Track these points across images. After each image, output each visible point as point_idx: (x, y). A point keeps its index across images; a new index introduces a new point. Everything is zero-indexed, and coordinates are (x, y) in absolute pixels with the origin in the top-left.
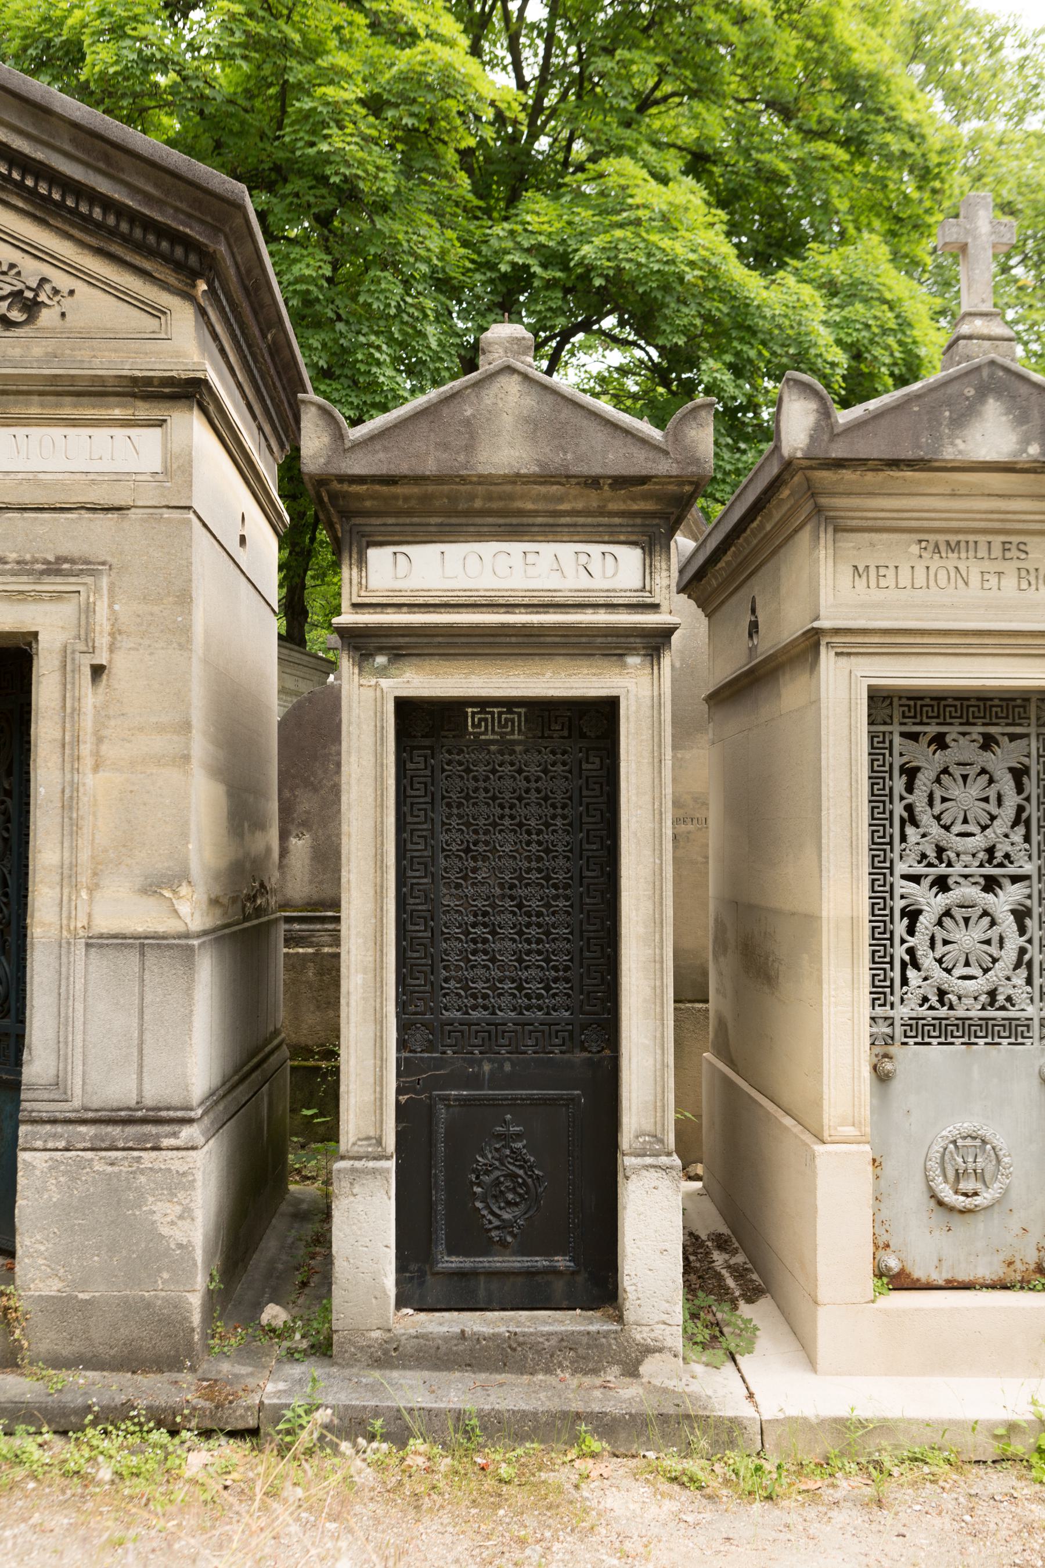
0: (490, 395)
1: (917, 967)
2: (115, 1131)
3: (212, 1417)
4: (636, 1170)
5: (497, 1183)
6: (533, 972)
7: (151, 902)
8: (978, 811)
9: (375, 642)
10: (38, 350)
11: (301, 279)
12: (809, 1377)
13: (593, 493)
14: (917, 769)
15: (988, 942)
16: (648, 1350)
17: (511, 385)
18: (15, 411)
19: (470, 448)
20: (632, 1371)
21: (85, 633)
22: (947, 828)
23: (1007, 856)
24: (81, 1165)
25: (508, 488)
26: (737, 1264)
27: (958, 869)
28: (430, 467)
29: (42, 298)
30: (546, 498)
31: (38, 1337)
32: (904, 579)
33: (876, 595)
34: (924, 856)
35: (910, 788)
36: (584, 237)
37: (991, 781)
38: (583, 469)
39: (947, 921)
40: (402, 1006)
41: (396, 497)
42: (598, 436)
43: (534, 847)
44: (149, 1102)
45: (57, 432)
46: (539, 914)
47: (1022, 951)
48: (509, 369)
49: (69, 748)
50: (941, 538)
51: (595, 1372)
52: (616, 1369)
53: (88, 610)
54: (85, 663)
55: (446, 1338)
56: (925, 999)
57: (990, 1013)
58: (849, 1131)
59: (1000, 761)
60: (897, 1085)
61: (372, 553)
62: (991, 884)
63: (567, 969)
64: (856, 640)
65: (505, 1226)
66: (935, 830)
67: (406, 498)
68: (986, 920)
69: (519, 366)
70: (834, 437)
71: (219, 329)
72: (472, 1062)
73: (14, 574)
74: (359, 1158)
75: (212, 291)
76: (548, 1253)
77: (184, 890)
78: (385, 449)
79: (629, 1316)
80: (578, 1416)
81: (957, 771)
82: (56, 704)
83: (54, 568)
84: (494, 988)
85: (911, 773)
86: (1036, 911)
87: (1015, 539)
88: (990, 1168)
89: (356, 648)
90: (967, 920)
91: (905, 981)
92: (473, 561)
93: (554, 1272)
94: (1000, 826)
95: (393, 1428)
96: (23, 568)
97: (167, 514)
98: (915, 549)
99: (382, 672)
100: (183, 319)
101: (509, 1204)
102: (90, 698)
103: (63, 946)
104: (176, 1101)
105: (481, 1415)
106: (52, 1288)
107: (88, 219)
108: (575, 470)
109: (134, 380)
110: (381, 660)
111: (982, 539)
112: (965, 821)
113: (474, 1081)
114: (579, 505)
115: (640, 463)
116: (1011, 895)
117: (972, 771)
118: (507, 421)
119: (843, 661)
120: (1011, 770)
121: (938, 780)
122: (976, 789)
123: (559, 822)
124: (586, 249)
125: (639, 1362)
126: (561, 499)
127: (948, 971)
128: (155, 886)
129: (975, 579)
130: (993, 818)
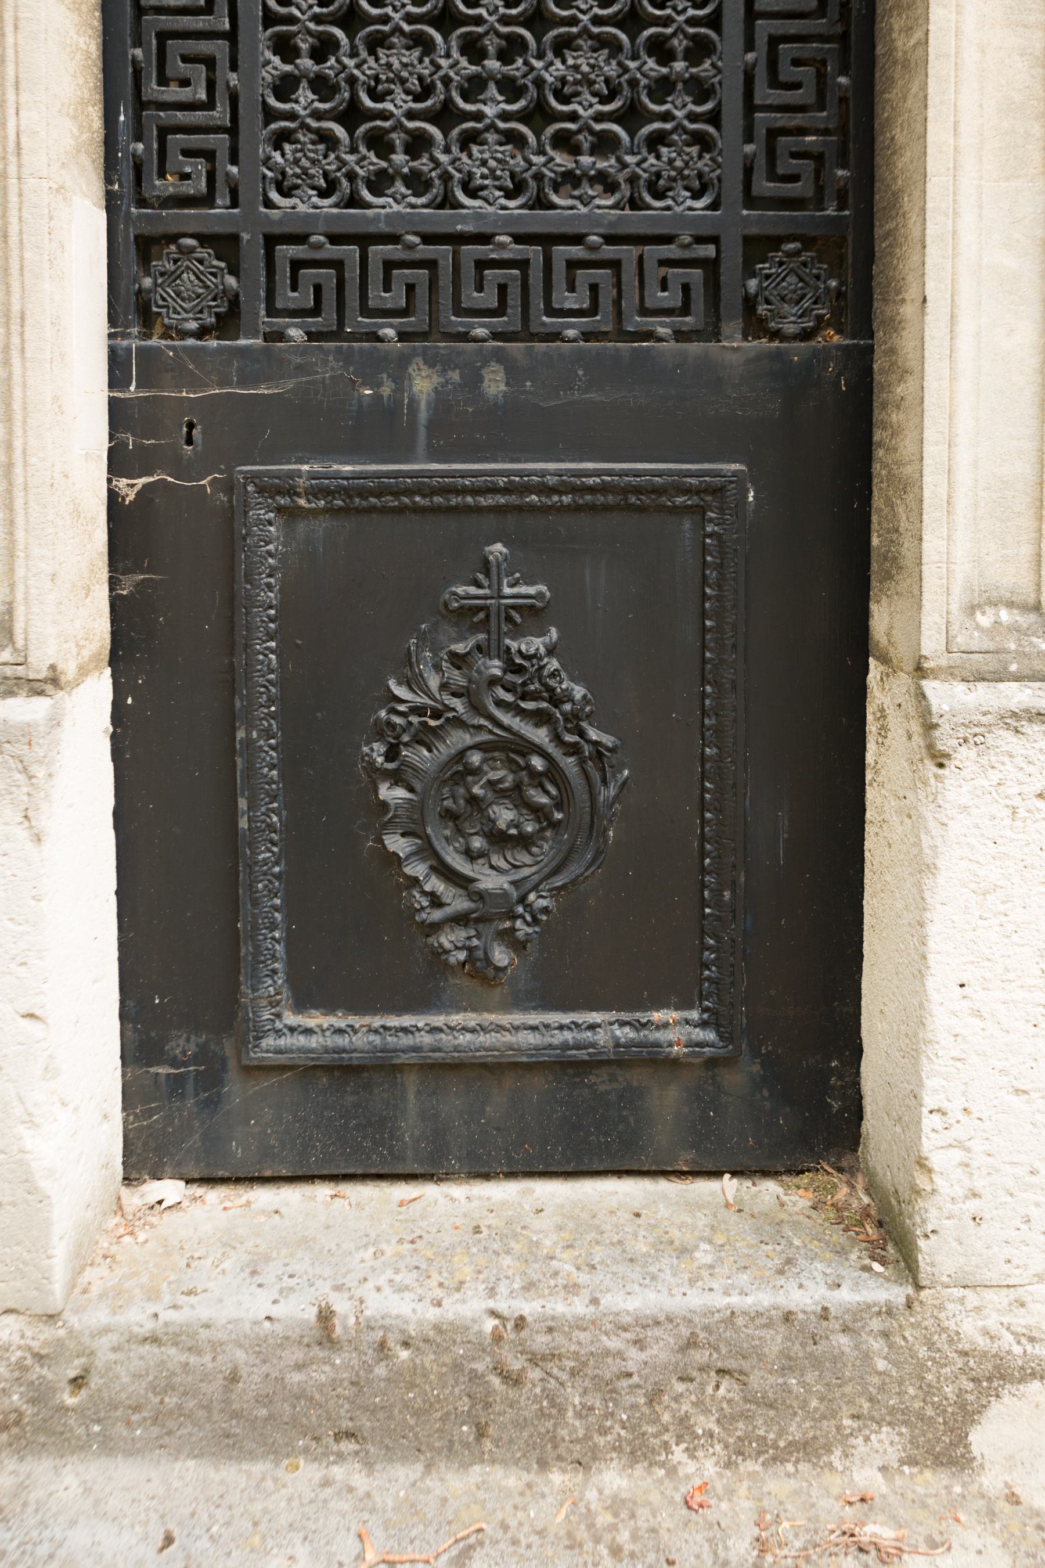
5: (458, 770)
65: (484, 913)
72: (372, 368)
76: (632, 996)
93: (654, 1060)
101: (499, 839)
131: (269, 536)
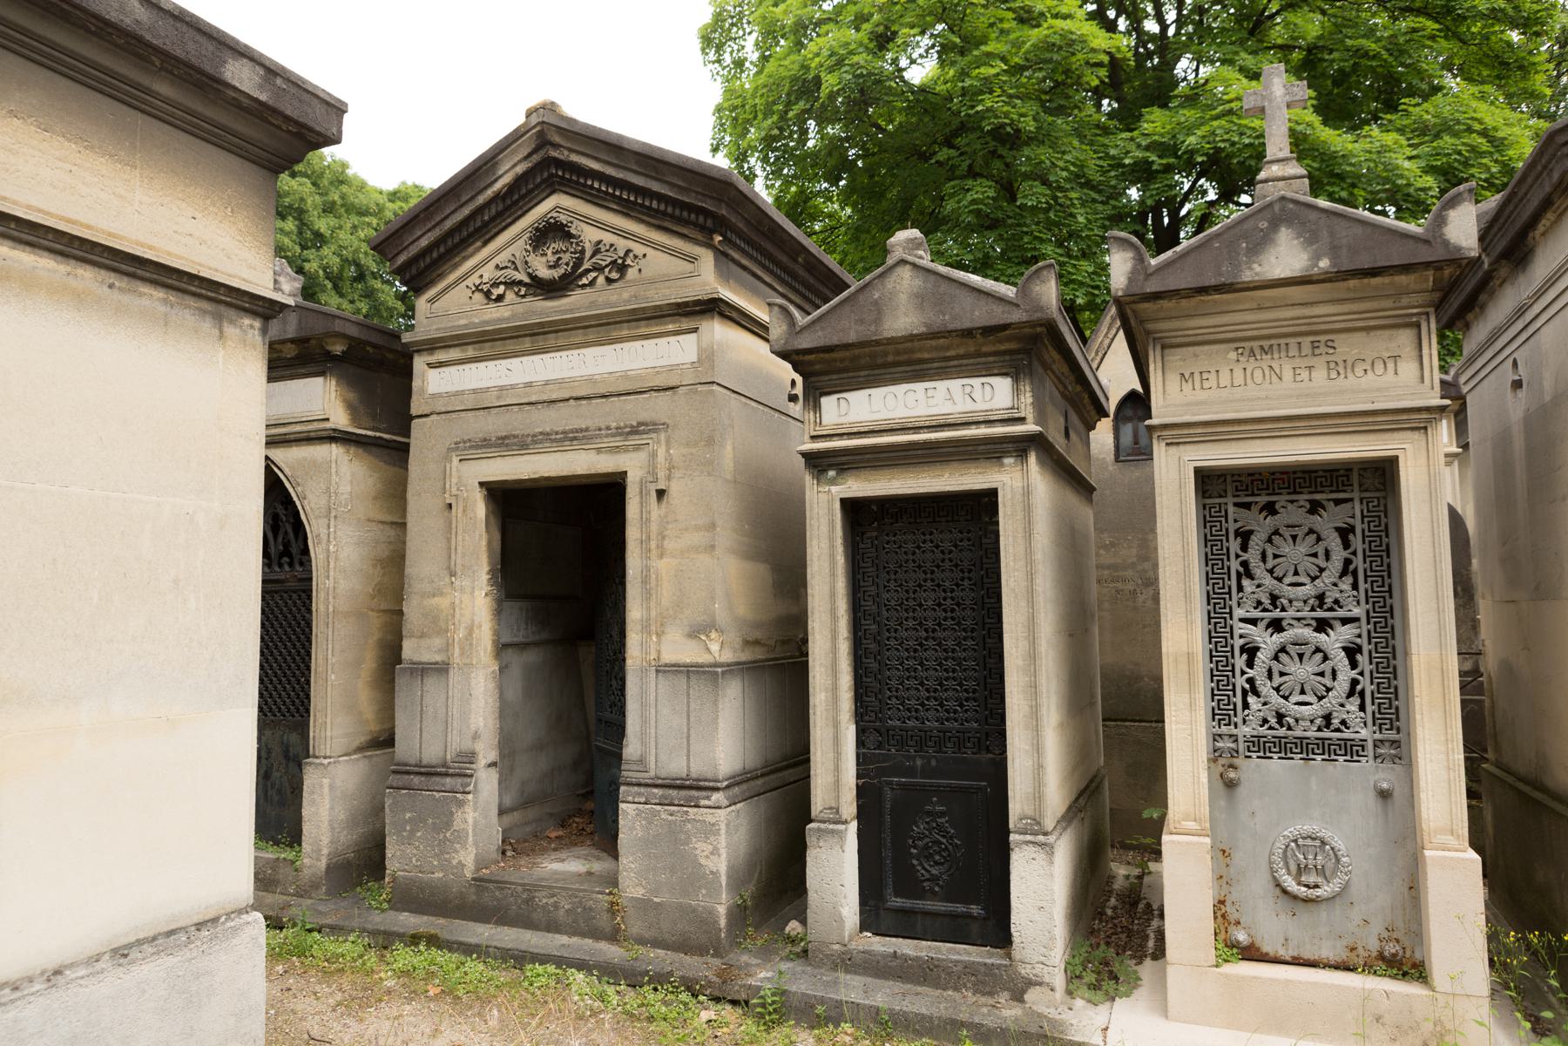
0: (890, 282)
1: (1257, 694)
2: (673, 793)
3: (720, 989)
5: (926, 847)
6: (951, 693)
7: (693, 644)
8: (1308, 565)
9: (826, 461)
10: (626, 295)
11: (974, 202)
12: (1161, 1021)
13: (970, 341)
14: (1251, 532)
15: (1322, 674)
16: (1030, 983)
17: (905, 273)
18: (615, 334)
19: (878, 321)
20: (1018, 997)
21: (652, 471)
22: (1280, 580)
23: (1336, 602)
24: (655, 814)
25: (909, 345)
26: (1118, 930)
27: (1291, 613)
28: (852, 337)
29: (628, 262)
30: (936, 348)
31: (635, 927)
32: (1225, 379)
33: (1202, 395)
34: (1259, 603)
35: (1244, 548)
36: (1190, 131)
37: (1319, 539)
38: (958, 325)
39: (1283, 656)
41: (835, 360)
42: (967, 299)
43: (949, 602)
44: (694, 775)
45: (638, 344)
46: (953, 651)
47: (1354, 682)
48: (903, 262)
49: (644, 542)
50: (1255, 344)
51: (991, 994)
52: (1006, 995)
53: (654, 455)
54: (653, 488)
55: (884, 956)
56: (1265, 721)
57: (1326, 734)
58: (1191, 825)
59: (1326, 523)
60: (1242, 791)
61: (825, 401)
62: (1322, 626)
63: (974, 691)
64: (1181, 433)
65: (934, 879)
66: (1268, 581)
67: (842, 360)
68: (1319, 656)
69: (910, 258)
70: (1148, 276)
71: (745, 262)
72: (909, 758)
73: (613, 435)
74: (824, 822)
75: (726, 240)
77: (713, 635)
78: (823, 329)
79: (1017, 951)
80: (963, 1024)
81: (1287, 533)
82: (637, 516)
83: (634, 431)
84: (922, 705)
85: (1245, 536)
86: (1366, 648)
87: (1323, 338)
88: (1330, 865)
89: (815, 467)
90: (1301, 656)
91: (1246, 706)
92: (890, 397)
93: (969, 916)
94: (1327, 578)
95: (833, 1014)
96: (619, 432)
97: (700, 388)
98: (1233, 355)
99: (833, 482)
100: (707, 259)
101: (936, 863)
102: (656, 511)
103: (643, 671)
104: (709, 776)
105: (891, 1013)
106: (639, 892)
107: (649, 208)
108: (951, 327)
109: (678, 305)
110: (832, 473)
111: (1292, 341)
112: (1296, 573)
113: (911, 772)
114: (962, 351)
115: (1000, 315)
116: (1340, 636)
117: (1300, 532)
118: (903, 297)
119: (1173, 449)
120: (1338, 529)
121: (1270, 541)
122: (1303, 548)
123: (966, 583)
124: (1192, 140)
125: (1024, 992)
126: (948, 348)
127: (1286, 698)
128: (697, 632)
129: (1287, 374)
130: (1322, 570)
131: (888, 794)
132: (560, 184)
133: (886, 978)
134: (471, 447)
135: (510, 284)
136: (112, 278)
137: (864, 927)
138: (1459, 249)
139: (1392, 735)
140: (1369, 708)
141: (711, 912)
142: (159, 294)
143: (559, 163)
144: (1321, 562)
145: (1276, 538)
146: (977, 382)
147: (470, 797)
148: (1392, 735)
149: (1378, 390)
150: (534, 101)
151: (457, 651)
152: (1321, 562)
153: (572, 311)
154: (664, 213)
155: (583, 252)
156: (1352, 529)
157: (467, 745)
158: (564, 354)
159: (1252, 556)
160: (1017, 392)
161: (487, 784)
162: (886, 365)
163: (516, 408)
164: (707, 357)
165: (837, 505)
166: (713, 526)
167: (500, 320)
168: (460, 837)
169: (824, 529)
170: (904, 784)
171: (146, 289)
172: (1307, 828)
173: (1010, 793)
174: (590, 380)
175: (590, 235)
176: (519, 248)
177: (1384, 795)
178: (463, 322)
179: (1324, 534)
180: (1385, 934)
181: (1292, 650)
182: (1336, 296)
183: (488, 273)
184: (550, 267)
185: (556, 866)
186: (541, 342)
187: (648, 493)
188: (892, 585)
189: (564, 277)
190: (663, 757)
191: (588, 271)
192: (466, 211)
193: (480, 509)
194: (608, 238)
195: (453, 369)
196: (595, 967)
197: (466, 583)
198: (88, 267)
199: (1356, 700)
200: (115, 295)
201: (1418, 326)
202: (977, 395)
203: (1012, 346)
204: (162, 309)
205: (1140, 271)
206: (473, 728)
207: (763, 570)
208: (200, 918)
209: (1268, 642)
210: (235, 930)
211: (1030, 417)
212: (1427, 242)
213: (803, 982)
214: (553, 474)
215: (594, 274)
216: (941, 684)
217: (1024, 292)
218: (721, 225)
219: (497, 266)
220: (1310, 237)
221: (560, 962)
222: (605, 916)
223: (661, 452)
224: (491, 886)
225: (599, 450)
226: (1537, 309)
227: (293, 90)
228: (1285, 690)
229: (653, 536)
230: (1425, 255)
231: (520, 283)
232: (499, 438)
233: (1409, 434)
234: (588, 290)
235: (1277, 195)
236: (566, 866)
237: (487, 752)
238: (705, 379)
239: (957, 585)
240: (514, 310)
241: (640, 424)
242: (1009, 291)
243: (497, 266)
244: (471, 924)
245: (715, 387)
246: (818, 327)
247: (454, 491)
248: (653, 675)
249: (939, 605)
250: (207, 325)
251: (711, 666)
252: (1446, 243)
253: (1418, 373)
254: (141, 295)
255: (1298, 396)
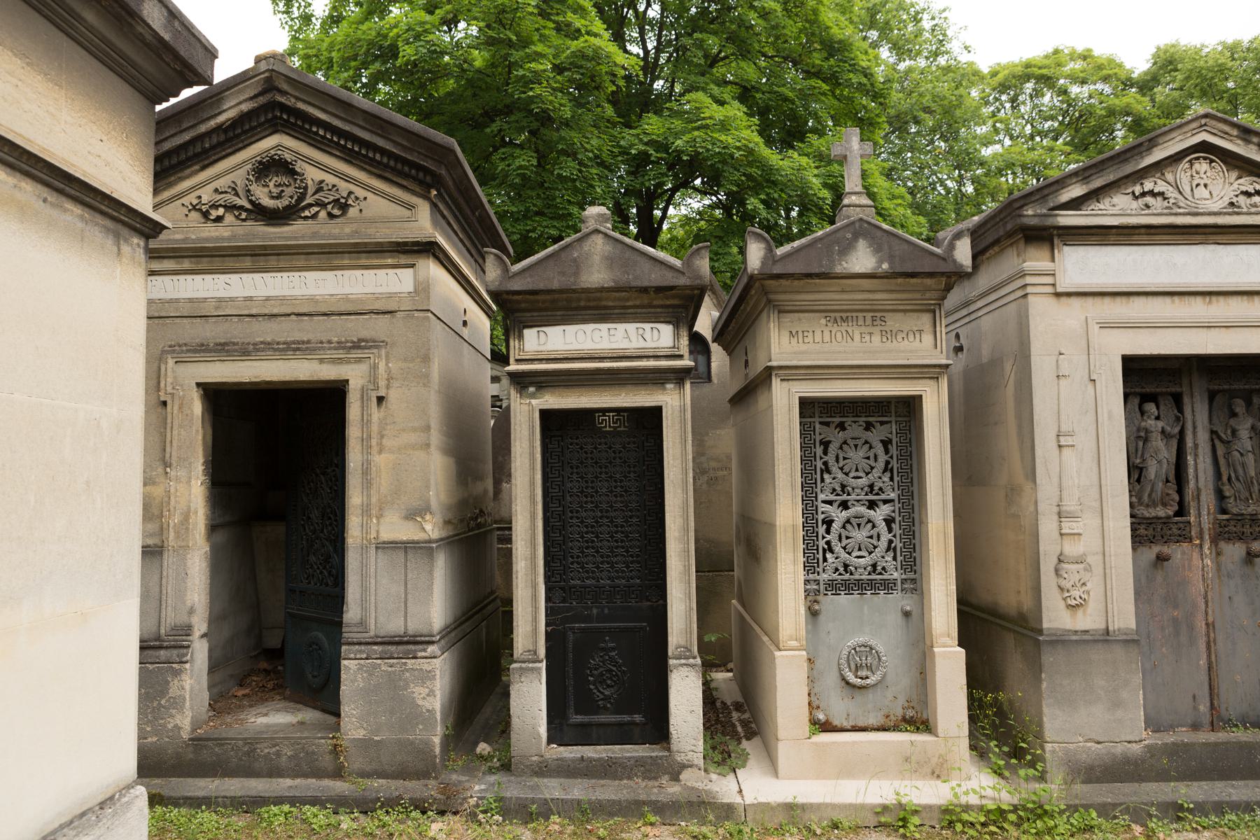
0: (587, 246)
1: (832, 551)
2: (392, 648)
3: (445, 804)
4: (676, 667)
5: (601, 674)
6: (619, 558)
7: (411, 523)
8: (864, 464)
9: (528, 380)
10: (347, 230)
11: (520, 167)
12: (774, 780)
13: (645, 296)
14: (830, 442)
15: (871, 537)
16: (684, 767)
17: (598, 240)
18: (336, 262)
19: (577, 273)
20: (675, 778)
21: (373, 379)
22: (847, 474)
23: (881, 489)
24: (375, 667)
25: (598, 295)
27: (853, 497)
28: (555, 285)
29: (350, 202)
30: (619, 299)
31: (354, 762)
32: (818, 338)
33: (803, 347)
34: (834, 490)
35: (825, 453)
36: (677, 135)
37: (871, 447)
38: (638, 283)
39: (848, 526)
40: (548, 579)
41: (538, 301)
42: (647, 265)
43: (619, 489)
44: (410, 632)
45: (358, 273)
46: (622, 526)
47: (890, 542)
48: (597, 231)
49: (365, 441)
50: (838, 315)
51: (655, 778)
52: (667, 777)
53: (375, 367)
54: (374, 395)
55: (573, 760)
56: (837, 570)
57: (874, 577)
58: (794, 643)
59: (875, 436)
60: (822, 618)
61: (526, 332)
62: (872, 505)
63: (638, 556)
64: (792, 372)
65: (606, 698)
66: (840, 475)
67: (544, 302)
68: (870, 525)
69: (602, 229)
70: (775, 262)
71: (445, 213)
73: (336, 349)
74: (524, 662)
75: (440, 195)
76: (631, 713)
77: (428, 517)
78: (531, 276)
79: (674, 747)
80: (644, 803)
81: (851, 443)
82: (359, 418)
83: (356, 346)
84: (598, 567)
85: (826, 445)
86: (898, 519)
87: (879, 315)
88: (875, 663)
89: (518, 383)
90: (859, 525)
91: (825, 560)
92: (580, 334)
93: (633, 723)
94: (876, 473)
95: (542, 810)
96: (341, 346)
97: (416, 314)
98: (823, 321)
99: (533, 396)
100: (424, 211)
101: (608, 686)
102: (376, 414)
103: (363, 549)
104: (425, 631)
105: (590, 802)
106: (360, 734)
107: (373, 160)
108: (634, 284)
109: (398, 244)
110: (532, 389)
111: (860, 315)
112: (857, 470)
113: (588, 619)
114: (638, 303)
115: (669, 279)
116: (884, 510)
117: (859, 442)
118: (597, 258)
119: (785, 384)
120: (882, 441)
121: (841, 448)
122: (862, 453)
123: (632, 475)
124: (679, 142)
125: (679, 773)
126: (628, 300)
127: (849, 554)
128: (412, 515)
129: (857, 337)
130: (872, 468)
131: (571, 637)
132: (283, 126)
133: (576, 778)
134: (188, 351)
135: (230, 208)
136: (45, 192)
137: (550, 741)
138: (962, 266)
139: (911, 575)
140: (899, 558)
141: (428, 743)
142: (78, 210)
143: (283, 108)
144: (872, 462)
145: (845, 446)
146: (647, 326)
147: (187, 666)
148: (911, 575)
149: (911, 351)
150: (263, 50)
151: (172, 535)
152: (872, 462)
153: (296, 238)
154: (386, 166)
155: (306, 188)
156: (890, 441)
157: (182, 619)
158: (285, 275)
159: (830, 458)
160: (677, 336)
161: (200, 652)
162: (576, 309)
163: (235, 319)
164: (422, 289)
165: (537, 415)
166: (427, 428)
167: (217, 239)
168: (177, 703)
169: (526, 433)
170: (584, 629)
171: (69, 205)
172: (862, 640)
173: (669, 630)
174: (312, 299)
175: (312, 175)
176: (240, 177)
177: (907, 614)
178: (178, 237)
179: (874, 444)
180: (906, 704)
181: (854, 521)
182: (889, 288)
183: (207, 195)
184: (273, 198)
185: (262, 720)
186: (261, 262)
187: (369, 399)
188: (575, 476)
189: (288, 207)
190: (381, 619)
191: (310, 205)
192: (187, 137)
193: (197, 407)
194: (330, 179)
195: (167, 278)
196: (327, 801)
197: (182, 473)
198: (29, 180)
199: (891, 554)
200: (48, 210)
201: (934, 312)
202: (648, 336)
203: (676, 302)
204: (80, 225)
205: (769, 257)
206: (189, 603)
207: (450, 461)
208: (100, 799)
209: (839, 516)
210: (129, 803)
211: (687, 355)
212: (944, 259)
213: (514, 789)
214: (275, 379)
215: (316, 209)
216: (582, 552)
217: (688, 263)
218: (437, 182)
219: (216, 190)
220: (877, 248)
221: (293, 801)
222: (328, 757)
223: (382, 365)
224: (210, 743)
225: (321, 361)
226: (979, 304)
227: (185, 33)
228: (849, 549)
229: (374, 435)
230: (943, 267)
231: (241, 208)
232: (217, 344)
233: (928, 381)
234: (310, 221)
235: (856, 217)
236: (274, 719)
237: (200, 625)
238: (420, 307)
239: (625, 477)
240: (230, 231)
241: (360, 340)
242: (678, 263)
243: (216, 190)
244: (190, 780)
245: (430, 314)
246: (527, 274)
247: (169, 389)
248: (373, 551)
249: (611, 492)
250: (109, 242)
251: (426, 542)
252: (955, 261)
253: (933, 342)
254: (66, 210)
255: (865, 352)
